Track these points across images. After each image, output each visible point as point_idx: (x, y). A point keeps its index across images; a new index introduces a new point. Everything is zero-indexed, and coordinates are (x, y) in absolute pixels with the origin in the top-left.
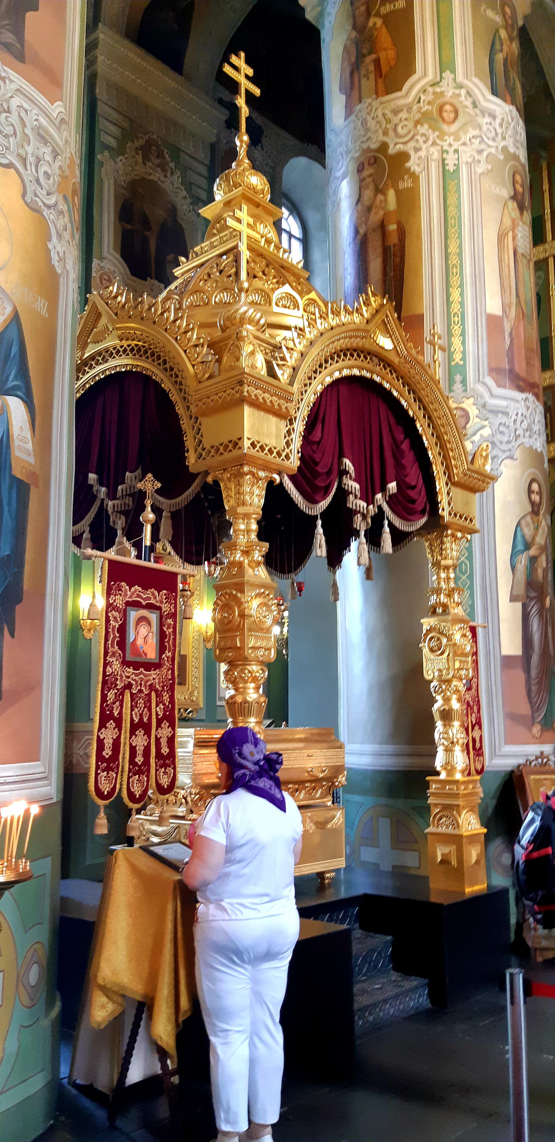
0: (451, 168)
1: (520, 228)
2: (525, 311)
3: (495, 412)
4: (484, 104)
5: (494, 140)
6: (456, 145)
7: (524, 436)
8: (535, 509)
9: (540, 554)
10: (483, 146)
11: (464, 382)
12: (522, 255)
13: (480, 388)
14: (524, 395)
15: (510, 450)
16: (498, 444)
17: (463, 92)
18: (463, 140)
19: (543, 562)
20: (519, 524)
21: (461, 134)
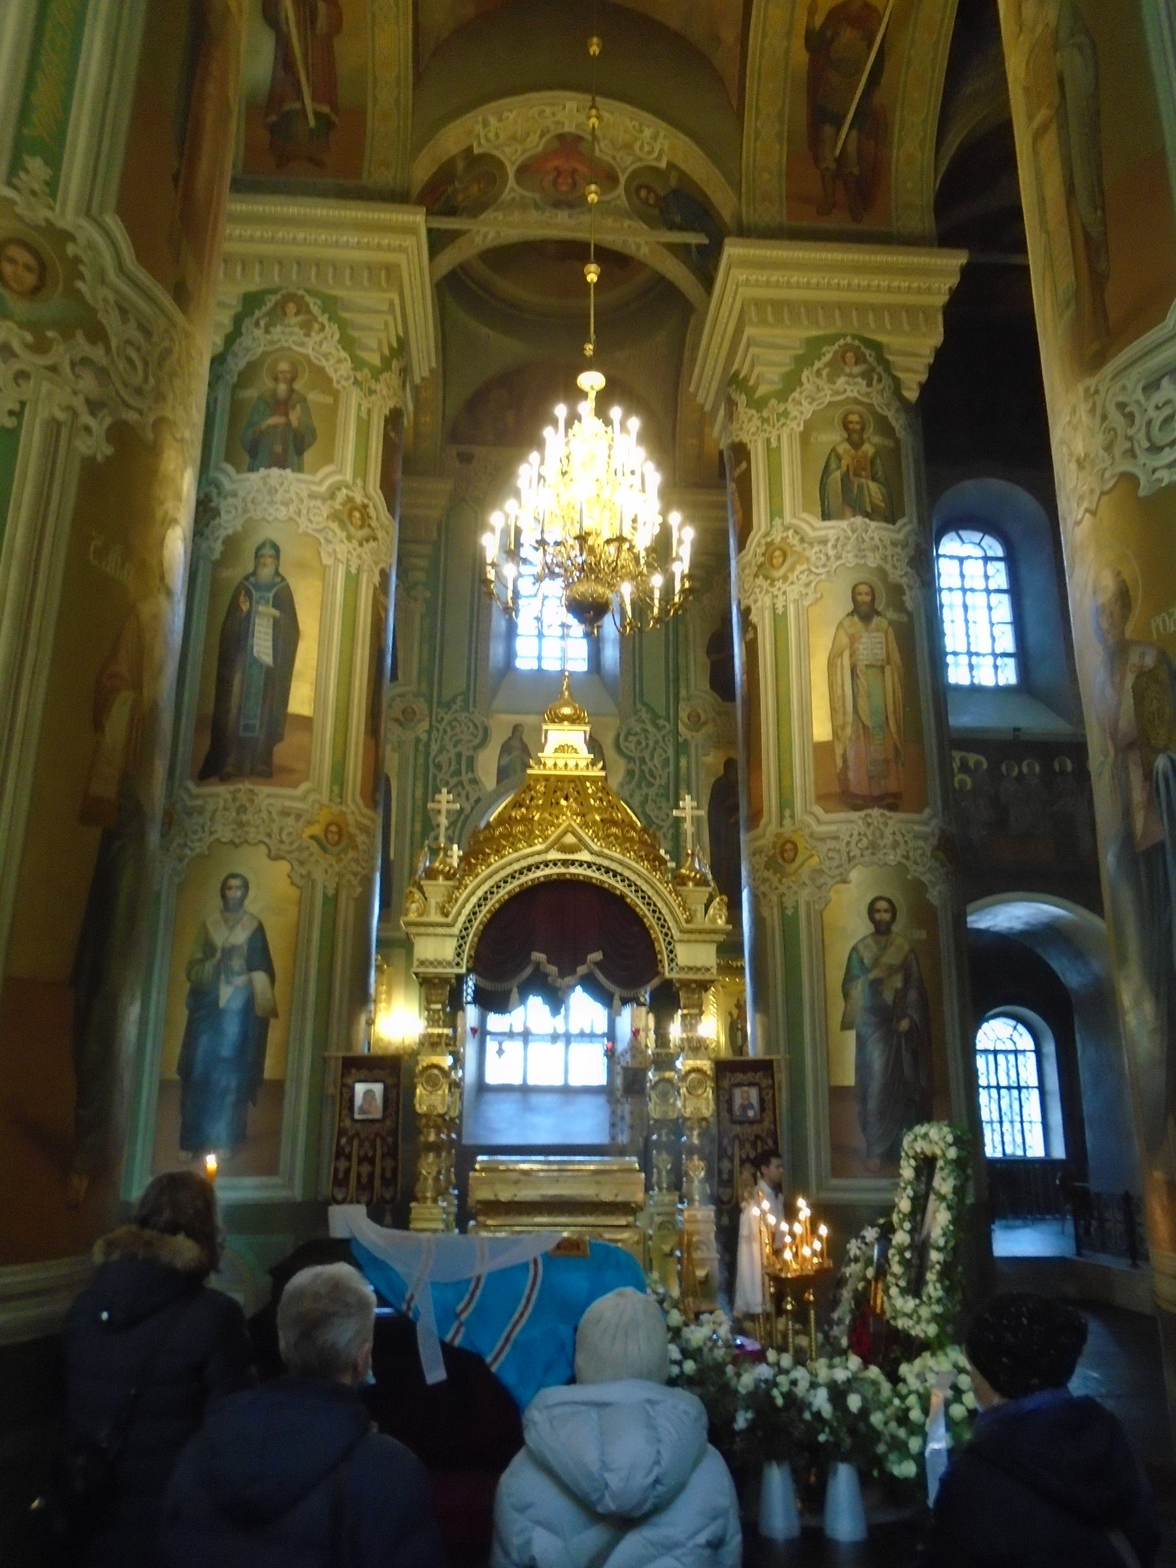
0: (780, 611)
1: (864, 640)
2: (869, 723)
3: (823, 839)
4: (812, 534)
5: (824, 566)
6: (784, 588)
7: (862, 856)
8: (882, 930)
9: (889, 976)
10: (812, 577)
11: (792, 817)
12: (867, 666)
13: (809, 819)
14: (862, 814)
15: (841, 874)
16: (827, 871)
17: (790, 533)
18: (790, 580)
19: (897, 982)
20: (854, 949)
21: (790, 575)
